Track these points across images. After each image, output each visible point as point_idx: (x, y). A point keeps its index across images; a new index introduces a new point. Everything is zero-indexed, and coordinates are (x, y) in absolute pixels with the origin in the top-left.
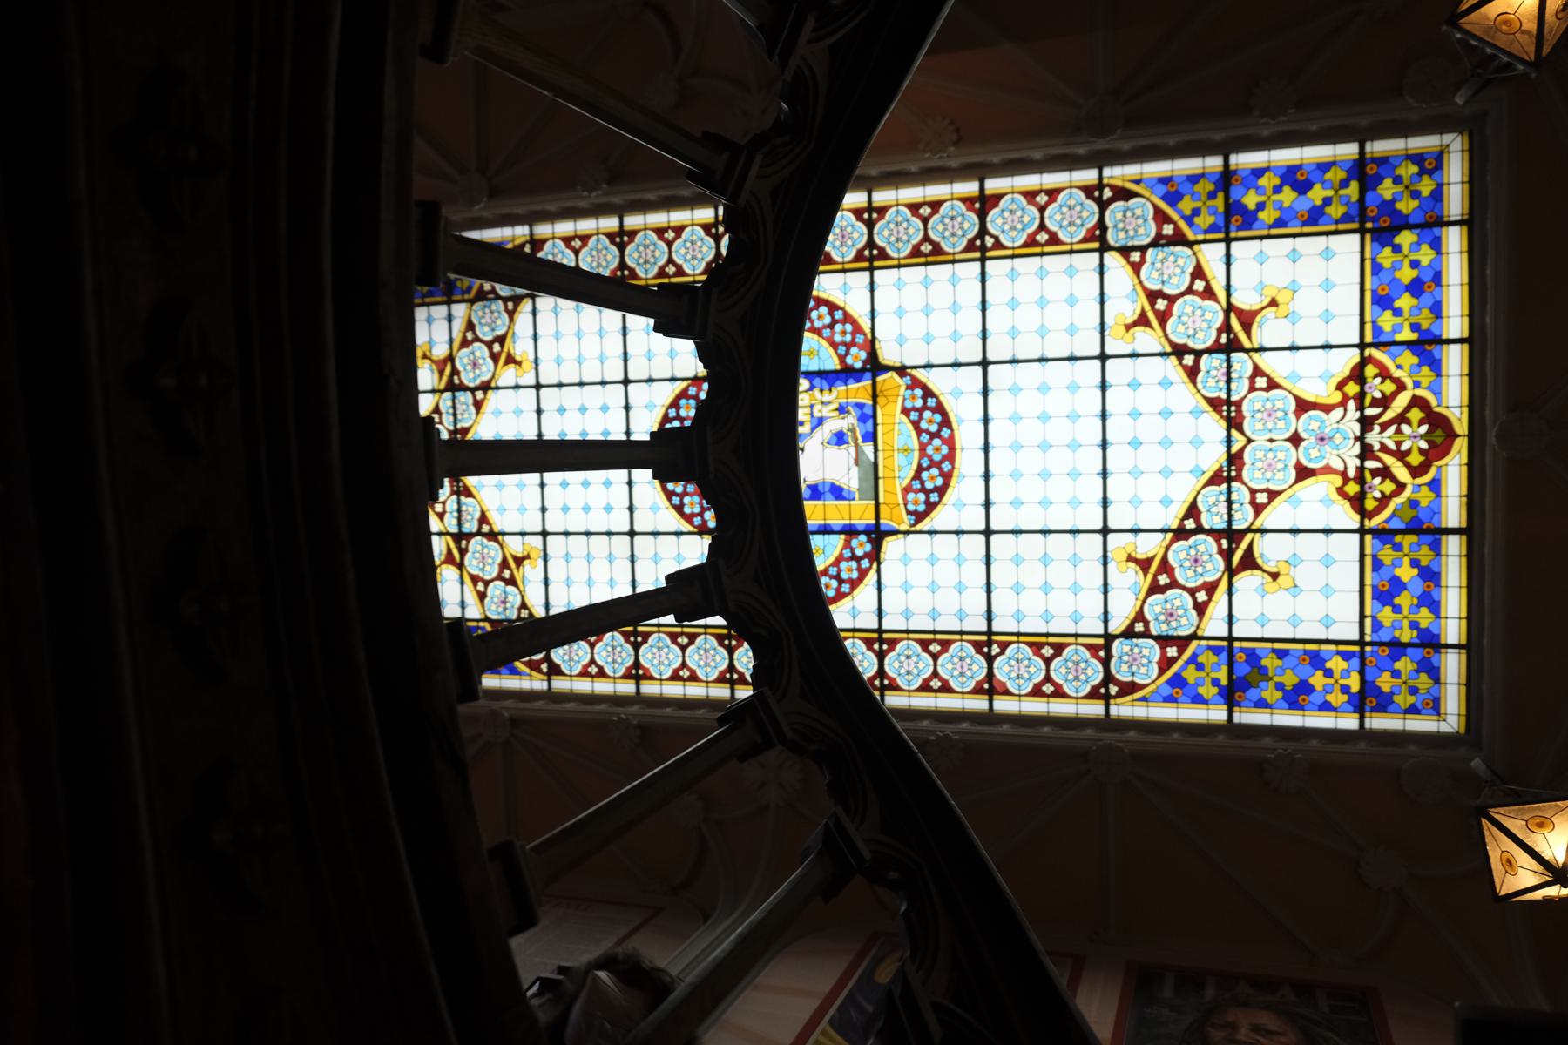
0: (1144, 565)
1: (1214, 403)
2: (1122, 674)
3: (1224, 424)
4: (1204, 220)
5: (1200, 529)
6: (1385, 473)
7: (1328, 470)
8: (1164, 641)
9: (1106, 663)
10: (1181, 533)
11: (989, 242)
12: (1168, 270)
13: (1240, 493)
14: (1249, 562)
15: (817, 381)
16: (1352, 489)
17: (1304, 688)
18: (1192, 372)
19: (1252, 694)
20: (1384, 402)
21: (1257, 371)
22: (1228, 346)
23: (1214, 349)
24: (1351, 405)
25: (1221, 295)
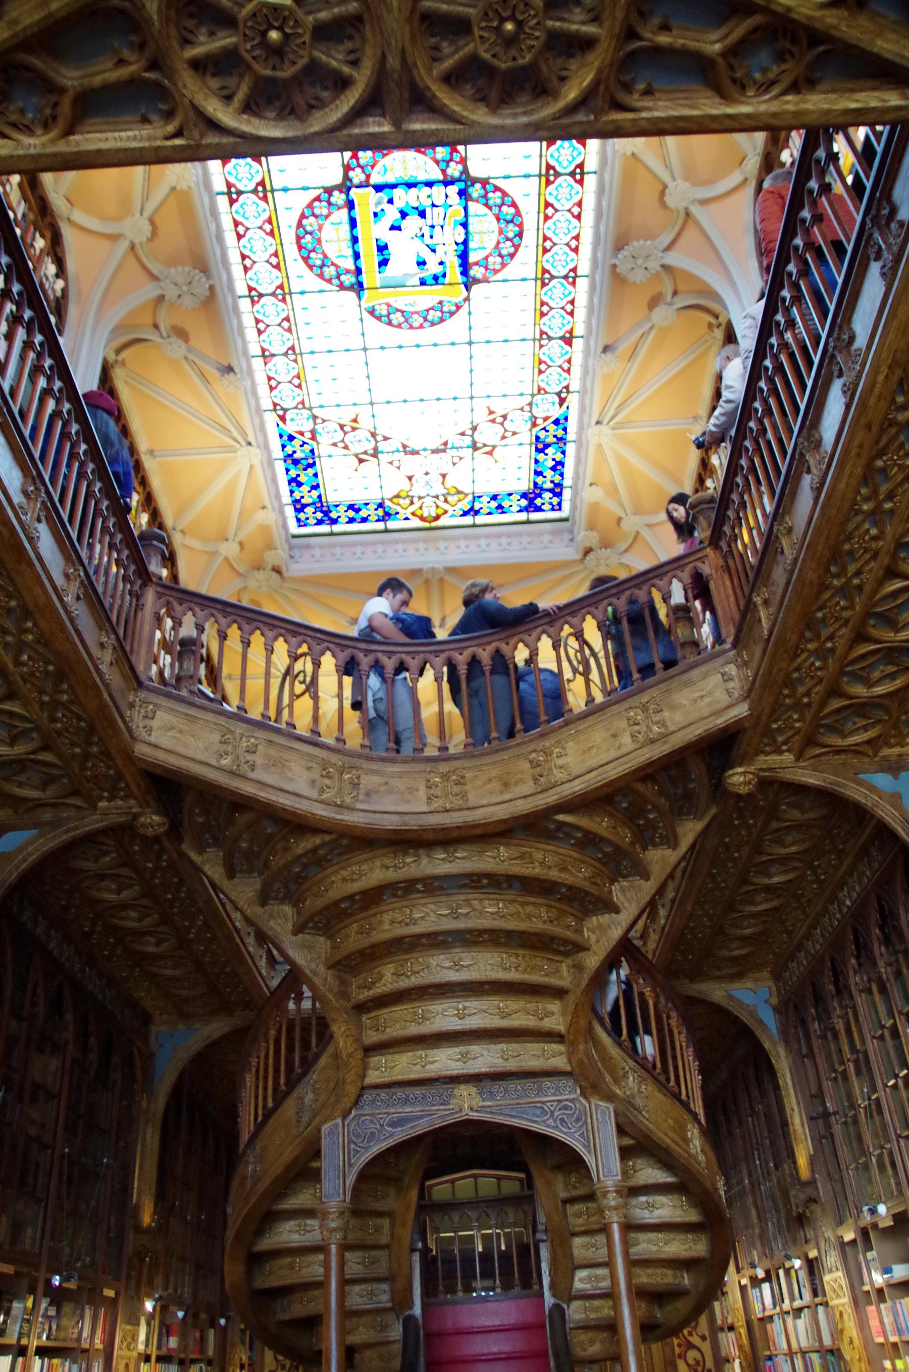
0: (355, 421)
1: (446, 444)
2: (288, 416)
3: (434, 447)
4: (542, 434)
5: (377, 442)
6: (412, 503)
7: (412, 485)
8: (313, 433)
9: (296, 408)
10: (374, 435)
11: (543, 342)
12: (520, 423)
13: (398, 456)
14: (361, 461)
15: (462, 247)
16: (403, 494)
17: (300, 484)
18: (463, 434)
19: (292, 467)
20: (446, 501)
21: (461, 458)
22: (475, 447)
23: (474, 443)
24: (445, 491)
25: (504, 442)
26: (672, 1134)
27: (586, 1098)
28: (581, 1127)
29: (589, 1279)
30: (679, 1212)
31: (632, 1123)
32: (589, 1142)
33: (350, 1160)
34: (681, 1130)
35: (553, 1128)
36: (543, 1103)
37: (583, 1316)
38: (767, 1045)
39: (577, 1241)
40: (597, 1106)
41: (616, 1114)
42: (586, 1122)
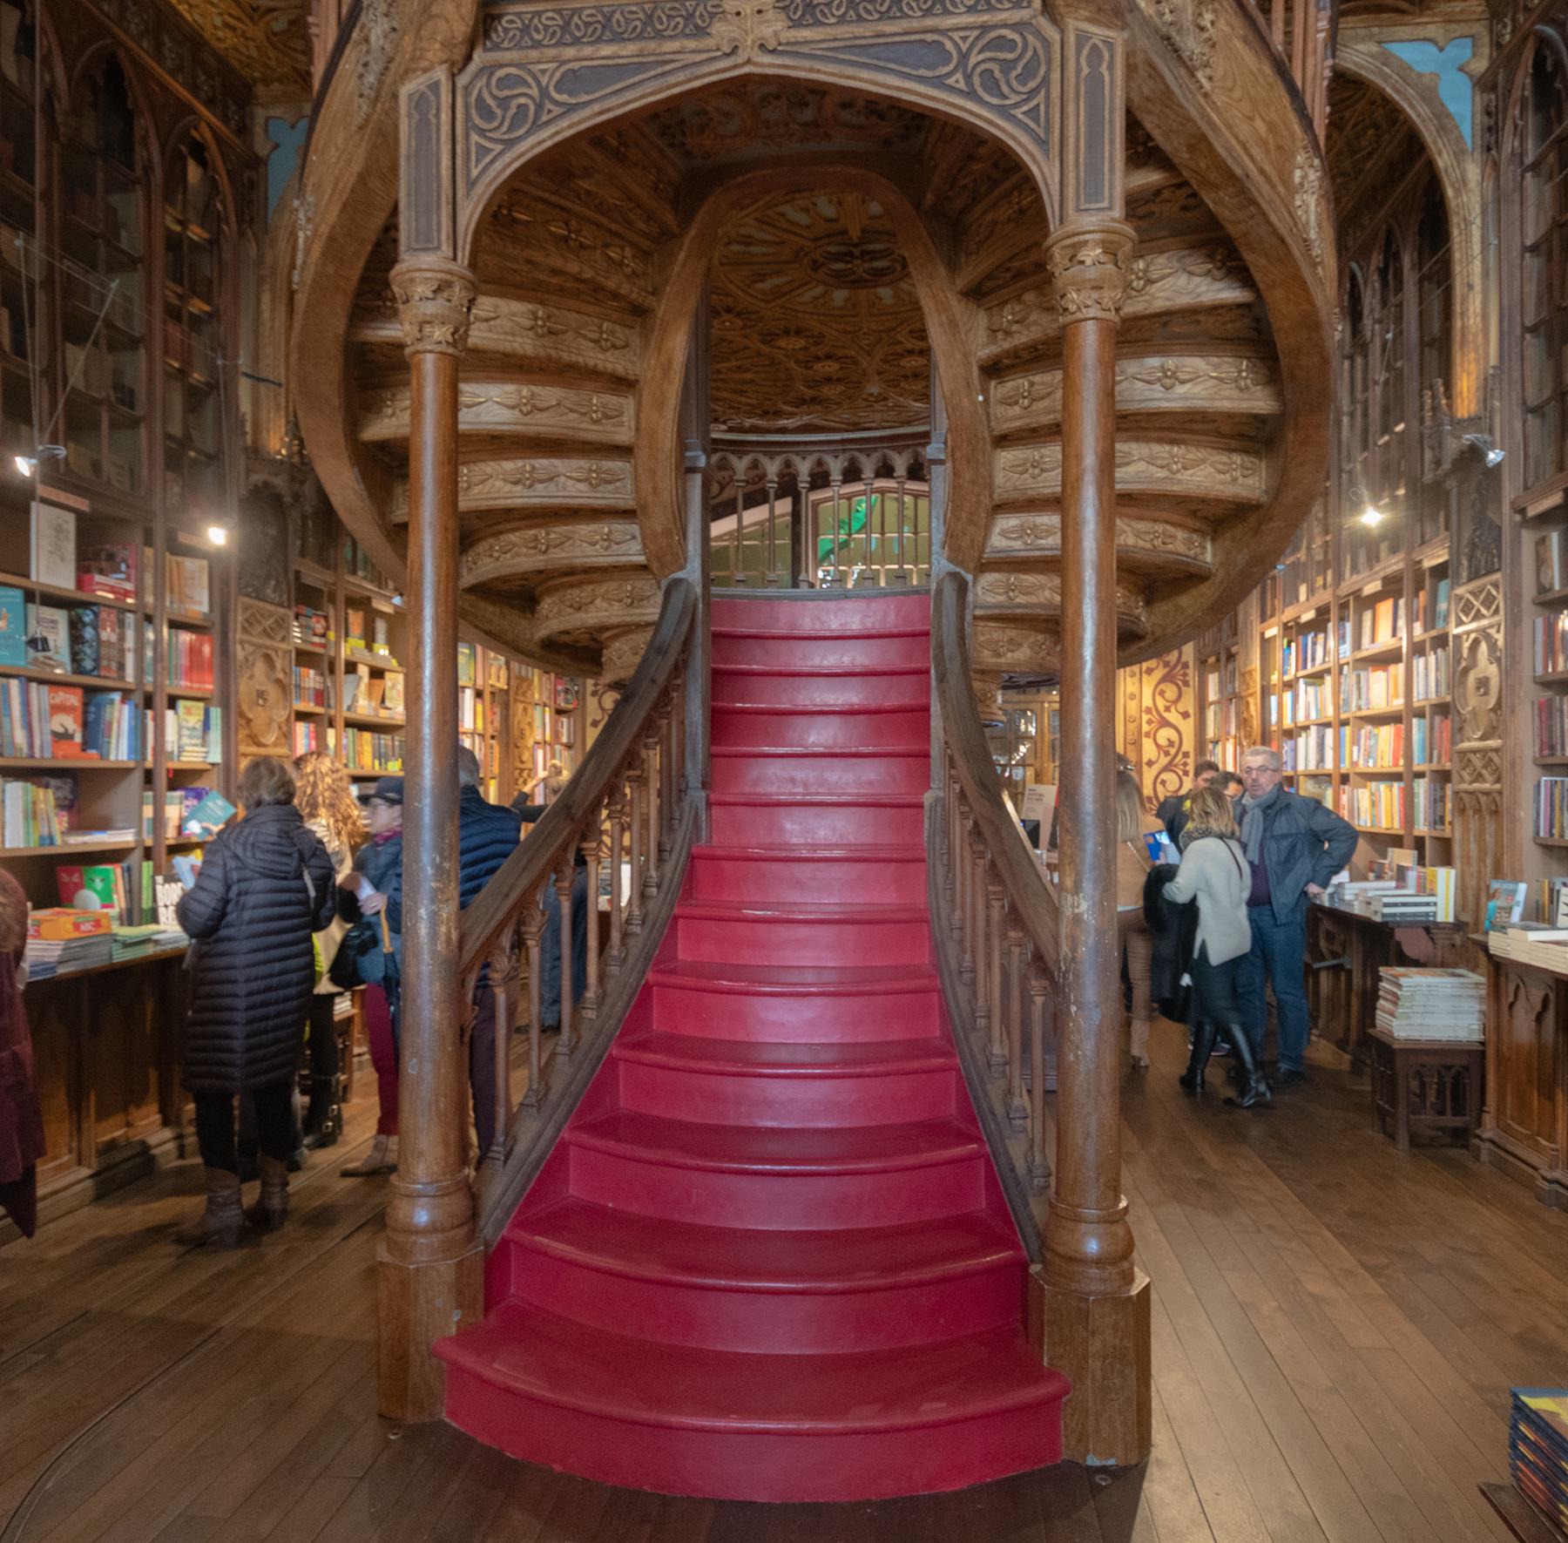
26: (1256, 152)
27: (1055, 20)
28: (1033, 93)
29: (1022, 531)
30: (1229, 391)
31: (1167, 95)
32: (1048, 129)
33: (468, 170)
34: (1284, 155)
35: (960, 92)
36: (944, 32)
37: (1001, 598)
38: (1443, 161)
39: (1006, 457)
40: (1082, 39)
41: (1131, 69)
42: (1046, 81)
